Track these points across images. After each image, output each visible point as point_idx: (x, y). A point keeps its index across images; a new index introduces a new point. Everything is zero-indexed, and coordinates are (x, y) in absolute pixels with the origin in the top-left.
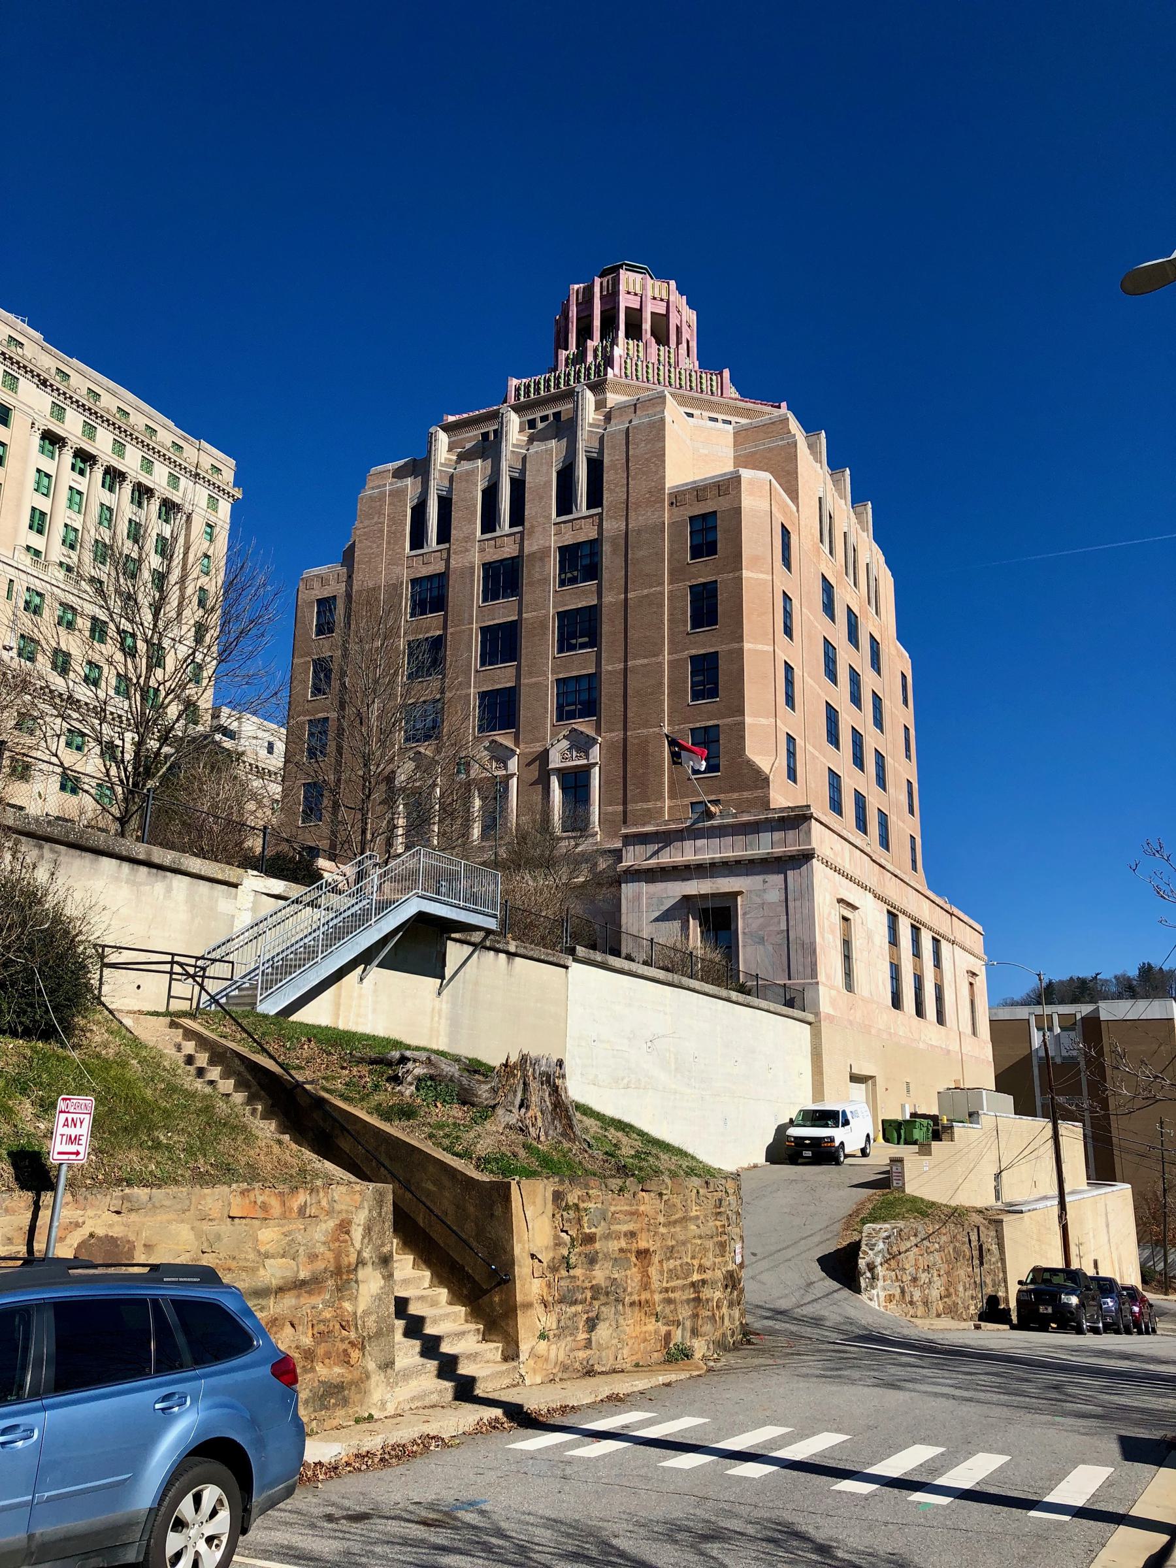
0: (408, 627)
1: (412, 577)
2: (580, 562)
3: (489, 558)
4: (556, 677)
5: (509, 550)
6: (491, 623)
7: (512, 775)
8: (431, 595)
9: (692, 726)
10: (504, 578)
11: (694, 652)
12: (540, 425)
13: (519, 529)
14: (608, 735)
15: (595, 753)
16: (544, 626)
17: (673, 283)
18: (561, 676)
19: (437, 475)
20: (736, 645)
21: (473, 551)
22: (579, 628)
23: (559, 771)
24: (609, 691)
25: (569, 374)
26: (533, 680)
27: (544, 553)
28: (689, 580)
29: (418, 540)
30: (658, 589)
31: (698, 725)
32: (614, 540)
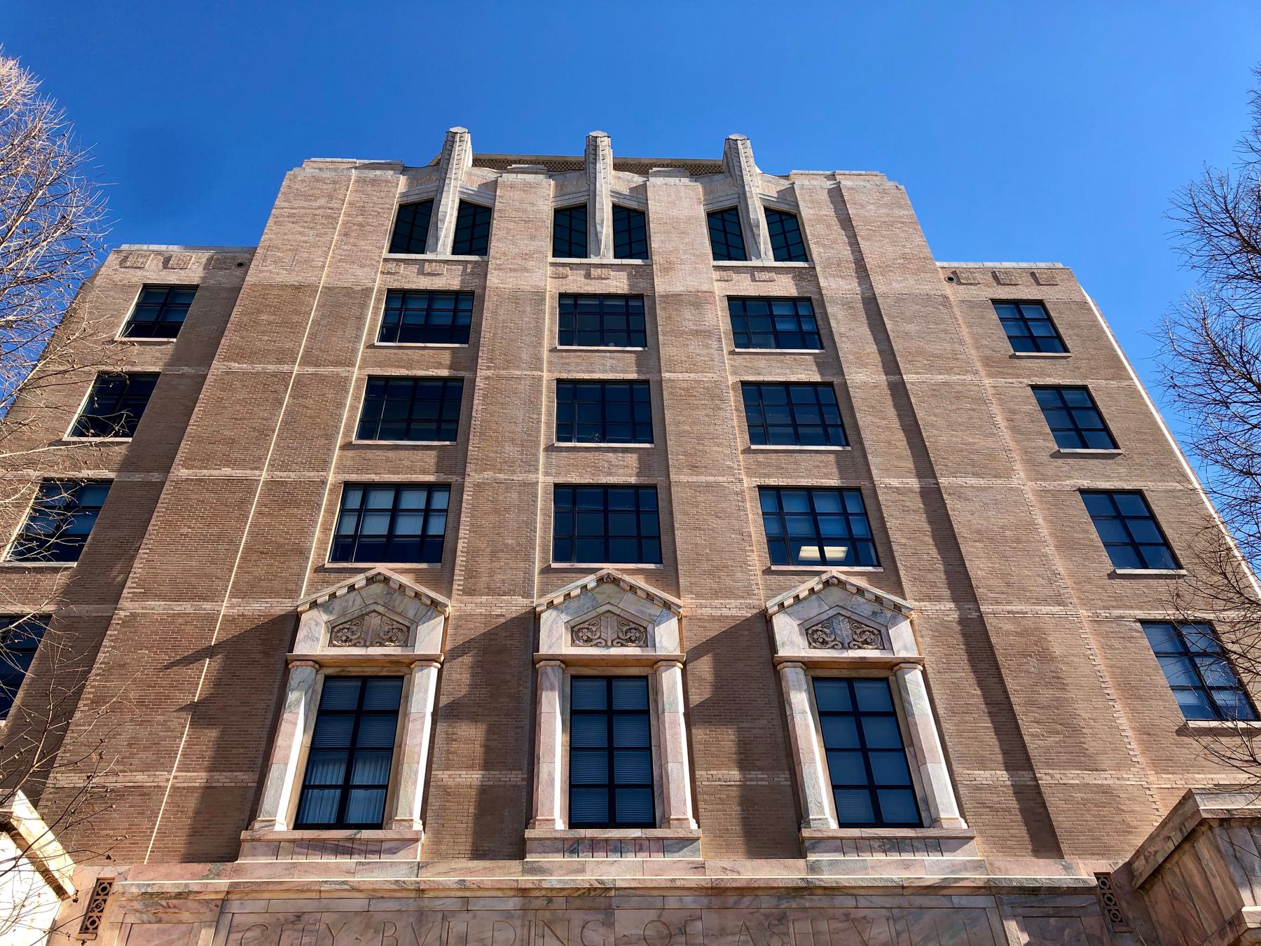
0: (368, 356)
3: (573, 289)
7: (670, 661)
9: (1141, 614)
15: (904, 642)
18: (772, 482)
26: (702, 479)
27: (698, 300)
28: (1029, 376)
30: (969, 377)
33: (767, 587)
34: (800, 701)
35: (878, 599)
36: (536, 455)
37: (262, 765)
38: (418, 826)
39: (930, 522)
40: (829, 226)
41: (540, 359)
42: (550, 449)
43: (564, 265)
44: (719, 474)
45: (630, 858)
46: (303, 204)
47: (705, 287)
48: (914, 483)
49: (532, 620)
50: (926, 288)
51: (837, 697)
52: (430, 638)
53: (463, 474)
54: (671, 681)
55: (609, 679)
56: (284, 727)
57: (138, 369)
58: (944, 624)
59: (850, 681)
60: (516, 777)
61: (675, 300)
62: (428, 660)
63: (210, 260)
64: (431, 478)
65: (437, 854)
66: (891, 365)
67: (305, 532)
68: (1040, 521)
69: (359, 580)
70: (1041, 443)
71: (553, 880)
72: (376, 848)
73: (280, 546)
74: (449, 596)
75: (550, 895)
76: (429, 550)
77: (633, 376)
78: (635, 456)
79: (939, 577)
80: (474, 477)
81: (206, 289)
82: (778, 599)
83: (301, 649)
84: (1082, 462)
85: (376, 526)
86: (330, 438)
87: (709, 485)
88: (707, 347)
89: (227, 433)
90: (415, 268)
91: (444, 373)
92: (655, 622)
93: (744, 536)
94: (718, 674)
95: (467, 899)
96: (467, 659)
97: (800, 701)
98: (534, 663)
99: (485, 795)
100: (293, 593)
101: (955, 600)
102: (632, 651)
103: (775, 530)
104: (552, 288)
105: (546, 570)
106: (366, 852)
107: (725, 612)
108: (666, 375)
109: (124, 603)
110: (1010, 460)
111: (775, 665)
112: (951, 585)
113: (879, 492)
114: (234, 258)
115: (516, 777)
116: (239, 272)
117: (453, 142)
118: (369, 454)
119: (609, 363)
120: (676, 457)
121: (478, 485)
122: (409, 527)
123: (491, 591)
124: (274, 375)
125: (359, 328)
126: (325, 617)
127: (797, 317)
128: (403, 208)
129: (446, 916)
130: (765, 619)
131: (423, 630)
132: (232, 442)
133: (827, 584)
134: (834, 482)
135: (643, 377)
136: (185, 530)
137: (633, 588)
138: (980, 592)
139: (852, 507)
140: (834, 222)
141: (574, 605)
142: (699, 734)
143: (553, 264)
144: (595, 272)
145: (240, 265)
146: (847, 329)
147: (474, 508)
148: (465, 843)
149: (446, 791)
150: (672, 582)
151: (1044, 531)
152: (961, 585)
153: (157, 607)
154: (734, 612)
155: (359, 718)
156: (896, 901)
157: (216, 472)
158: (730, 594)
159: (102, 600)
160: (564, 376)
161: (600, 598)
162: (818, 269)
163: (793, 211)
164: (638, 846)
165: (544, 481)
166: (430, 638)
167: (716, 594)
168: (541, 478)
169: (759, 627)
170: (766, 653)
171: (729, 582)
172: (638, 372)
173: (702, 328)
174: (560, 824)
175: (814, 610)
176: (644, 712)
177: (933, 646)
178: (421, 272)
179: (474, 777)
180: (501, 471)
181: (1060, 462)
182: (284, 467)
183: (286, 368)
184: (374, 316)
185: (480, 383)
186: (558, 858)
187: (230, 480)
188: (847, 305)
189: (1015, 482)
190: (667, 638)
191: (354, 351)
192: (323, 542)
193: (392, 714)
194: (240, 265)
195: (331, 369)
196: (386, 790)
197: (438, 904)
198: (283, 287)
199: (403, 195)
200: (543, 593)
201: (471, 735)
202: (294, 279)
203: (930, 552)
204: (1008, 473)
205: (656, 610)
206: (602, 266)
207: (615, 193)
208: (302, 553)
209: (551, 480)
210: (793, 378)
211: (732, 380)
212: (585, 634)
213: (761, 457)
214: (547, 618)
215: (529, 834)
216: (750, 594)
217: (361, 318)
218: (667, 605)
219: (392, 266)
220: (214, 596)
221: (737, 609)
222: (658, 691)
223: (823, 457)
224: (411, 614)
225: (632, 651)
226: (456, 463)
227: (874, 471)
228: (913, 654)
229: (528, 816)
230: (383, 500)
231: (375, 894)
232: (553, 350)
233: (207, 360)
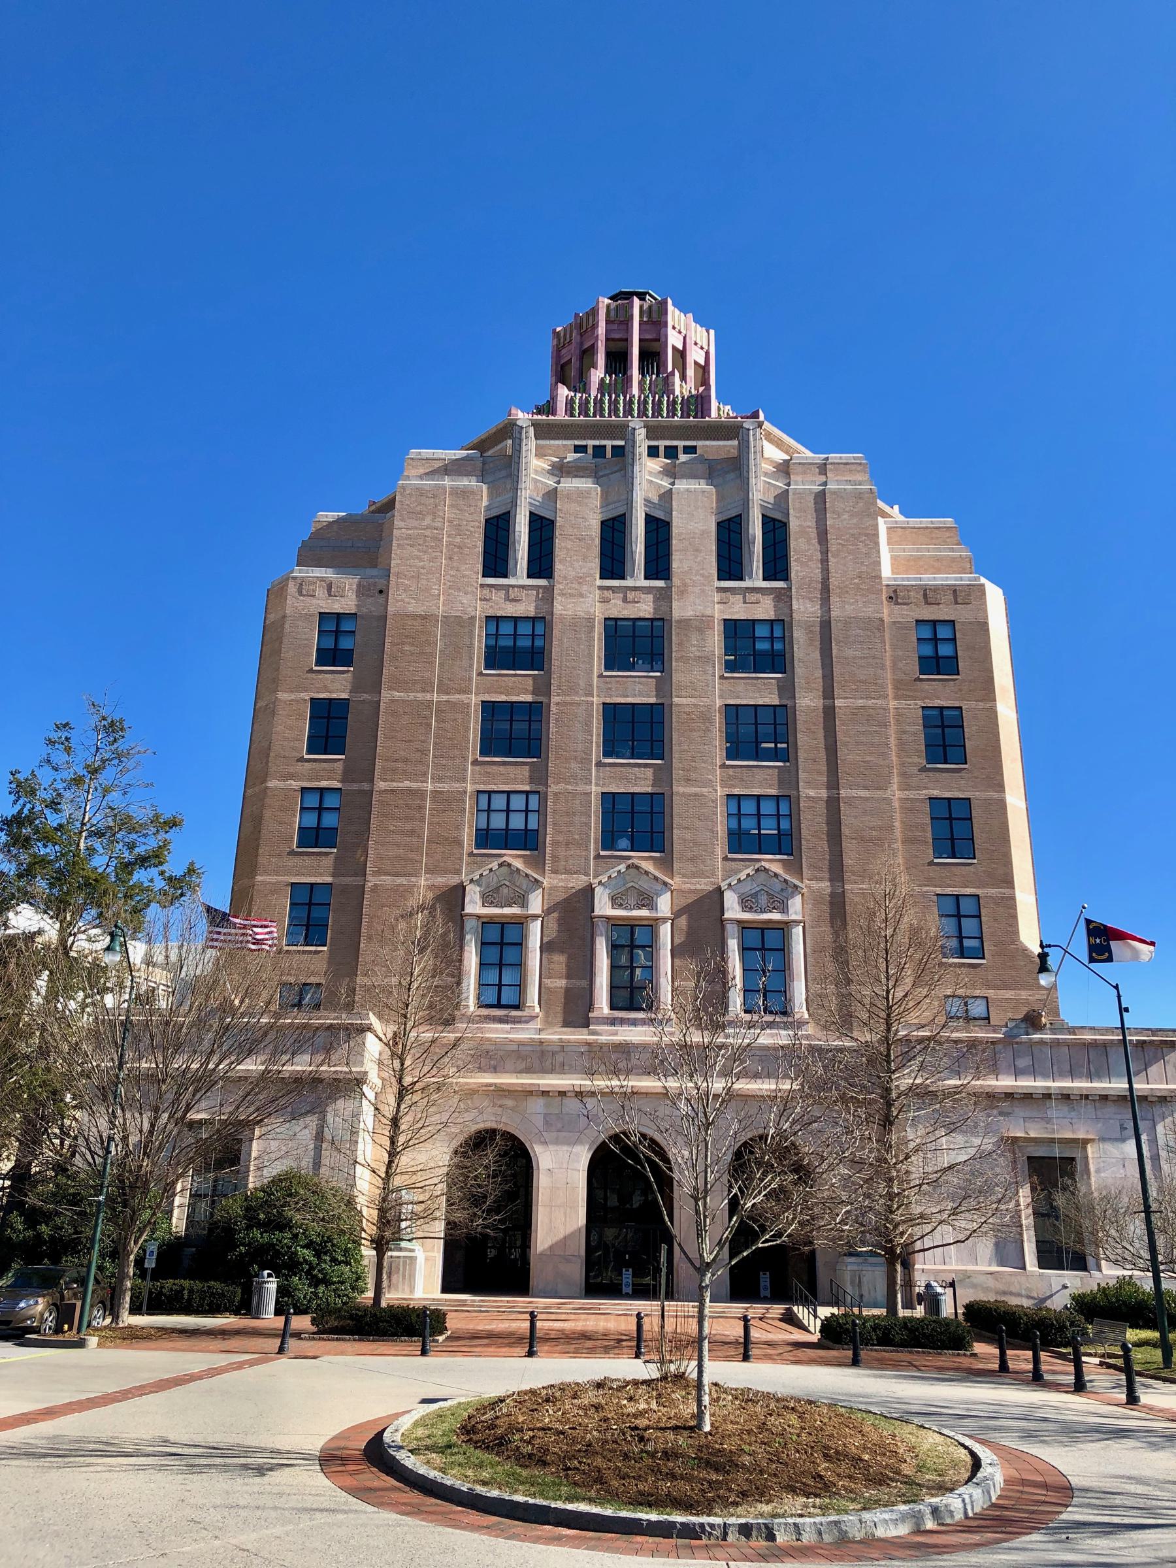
1: (491, 613)
2: (754, 647)
3: (615, 614)
4: (727, 791)
5: (645, 608)
6: (622, 700)
7: (665, 919)
8: (519, 646)
9: (939, 890)
10: (636, 644)
11: (935, 793)
12: (683, 458)
13: (660, 583)
14: (815, 885)
15: (796, 908)
16: (707, 719)
17: (712, 332)
18: (736, 791)
19: (530, 485)
20: (995, 796)
21: (584, 599)
22: (756, 734)
23: (743, 926)
24: (812, 826)
25: (645, 402)
27: (702, 624)
28: (923, 699)
29: (496, 561)
30: (880, 702)
31: (948, 891)
32: (808, 628)
33: (724, 870)
34: (733, 944)
35: (786, 881)
36: (590, 770)
37: (458, 977)
38: (537, 1010)
39: (828, 824)
40: (808, 542)
41: (591, 686)
42: (599, 764)
43: (608, 588)
44: (706, 783)
45: (640, 1028)
46: (415, 523)
47: (708, 612)
48: (823, 793)
49: (589, 891)
50: (869, 611)
51: (754, 939)
52: (536, 904)
53: (547, 786)
54: (665, 930)
55: (632, 926)
56: (466, 955)
57: (334, 696)
58: (821, 896)
59: (763, 929)
60: (584, 983)
61: (685, 623)
62: (536, 917)
63: (359, 585)
64: (527, 788)
65: (548, 1023)
66: (829, 692)
67: (459, 829)
68: (897, 824)
69: (494, 865)
70: (916, 759)
71: (603, 1039)
72: (518, 1020)
73: (447, 839)
74: (543, 874)
75: (601, 1046)
76: (529, 840)
77: (653, 700)
78: (651, 770)
79: (825, 865)
80: (553, 789)
81: (362, 617)
82: (727, 882)
83: (469, 909)
84: (937, 775)
85: (498, 822)
86: (465, 758)
87: (696, 796)
88: (705, 672)
89: (402, 753)
90: (502, 593)
91: (529, 698)
92: (658, 895)
93: (714, 832)
94: (690, 926)
95: (563, 1046)
96: (555, 915)
97: (733, 944)
98: (592, 918)
99: (568, 991)
100: (458, 872)
101: (831, 880)
102: (644, 913)
103: (734, 825)
104: (599, 612)
105: (598, 857)
106: (514, 1022)
107: (698, 887)
108: (675, 700)
109: (369, 877)
110: (890, 775)
111: (722, 922)
112: (831, 869)
113: (801, 800)
114: (375, 584)
115: (584, 983)
116: (381, 599)
117: (521, 440)
118: (490, 769)
119: (638, 687)
120: (677, 774)
121: (556, 794)
122: (517, 822)
123: (567, 872)
124: (422, 702)
125: (471, 658)
126: (478, 889)
127: (772, 638)
128: (487, 521)
129: (554, 1053)
130: (720, 892)
131: (532, 897)
132: (406, 760)
133: (757, 870)
134: (774, 792)
135: (659, 701)
136: (392, 828)
137: (646, 873)
138: (846, 875)
139: (784, 810)
140: (814, 535)
141: (613, 882)
142: (677, 962)
143: (600, 588)
144: (631, 595)
145: (381, 592)
146: (804, 653)
147: (554, 812)
148: (560, 1018)
149: (549, 988)
150: (667, 864)
151: (898, 834)
152: (837, 872)
153: (387, 880)
154: (703, 887)
155: (503, 943)
156: (764, 1053)
157: (401, 785)
158: (702, 874)
159: (356, 875)
160: (608, 700)
161: (627, 877)
162: (793, 590)
163: (784, 520)
164: (643, 1022)
165: (595, 790)
166: (536, 904)
167: (694, 875)
168: (594, 788)
169: (716, 897)
170: (719, 914)
171: (702, 867)
172: (657, 696)
173: (702, 654)
174: (606, 1010)
175: (748, 888)
176: (651, 947)
177: (812, 910)
178: (507, 599)
179: (562, 983)
180: (568, 783)
181: (924, 775)
182: (440, 781)
183: (428, 696)
184: (479, 647)
185: (553, 708)
186: (606, 1028)
187: (410, 791)
188: (808, 628)
189: (888, 794)
190: (664, 905)
191: (470, 679)
192: (470, 835)
193: (520, 944)
194: (381, 592)
195: (457, 696)
196: (520, 986)
197: (549, 1048)
198: (415, 617)
199: (488, 508)
200: (595, 877)
201: (560, 960)
202: (420, 610)
203: (823, 848)
204: (883, 785)
205: (659, 887)
206: (635, 589)
207: (647, 501)
208: (460, 844)
209: (600, 790)
210: (761, 703)
211: (719, 703)
212: (619, 901)
213: (731, 772)
214: (598, 891)
215: (591, 1015)
216: (714, 875)
217: (471, 648)
218: (665, 884)
219: (486, 591)
220: (416, 874)
221: (704, 885)
222: (657, 936)
223: (770, 771)
224: (524, 887)
225: (644, 913)
226: (540, 776)
227: (801, 784)
228: (799, 917)
229: (590, 1006)
230: (499, 802)
231: (521, 1043)
232: (600, 676)
233: (377, 687)
